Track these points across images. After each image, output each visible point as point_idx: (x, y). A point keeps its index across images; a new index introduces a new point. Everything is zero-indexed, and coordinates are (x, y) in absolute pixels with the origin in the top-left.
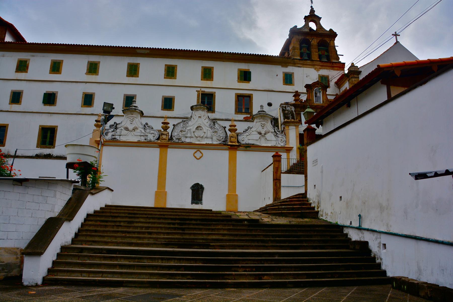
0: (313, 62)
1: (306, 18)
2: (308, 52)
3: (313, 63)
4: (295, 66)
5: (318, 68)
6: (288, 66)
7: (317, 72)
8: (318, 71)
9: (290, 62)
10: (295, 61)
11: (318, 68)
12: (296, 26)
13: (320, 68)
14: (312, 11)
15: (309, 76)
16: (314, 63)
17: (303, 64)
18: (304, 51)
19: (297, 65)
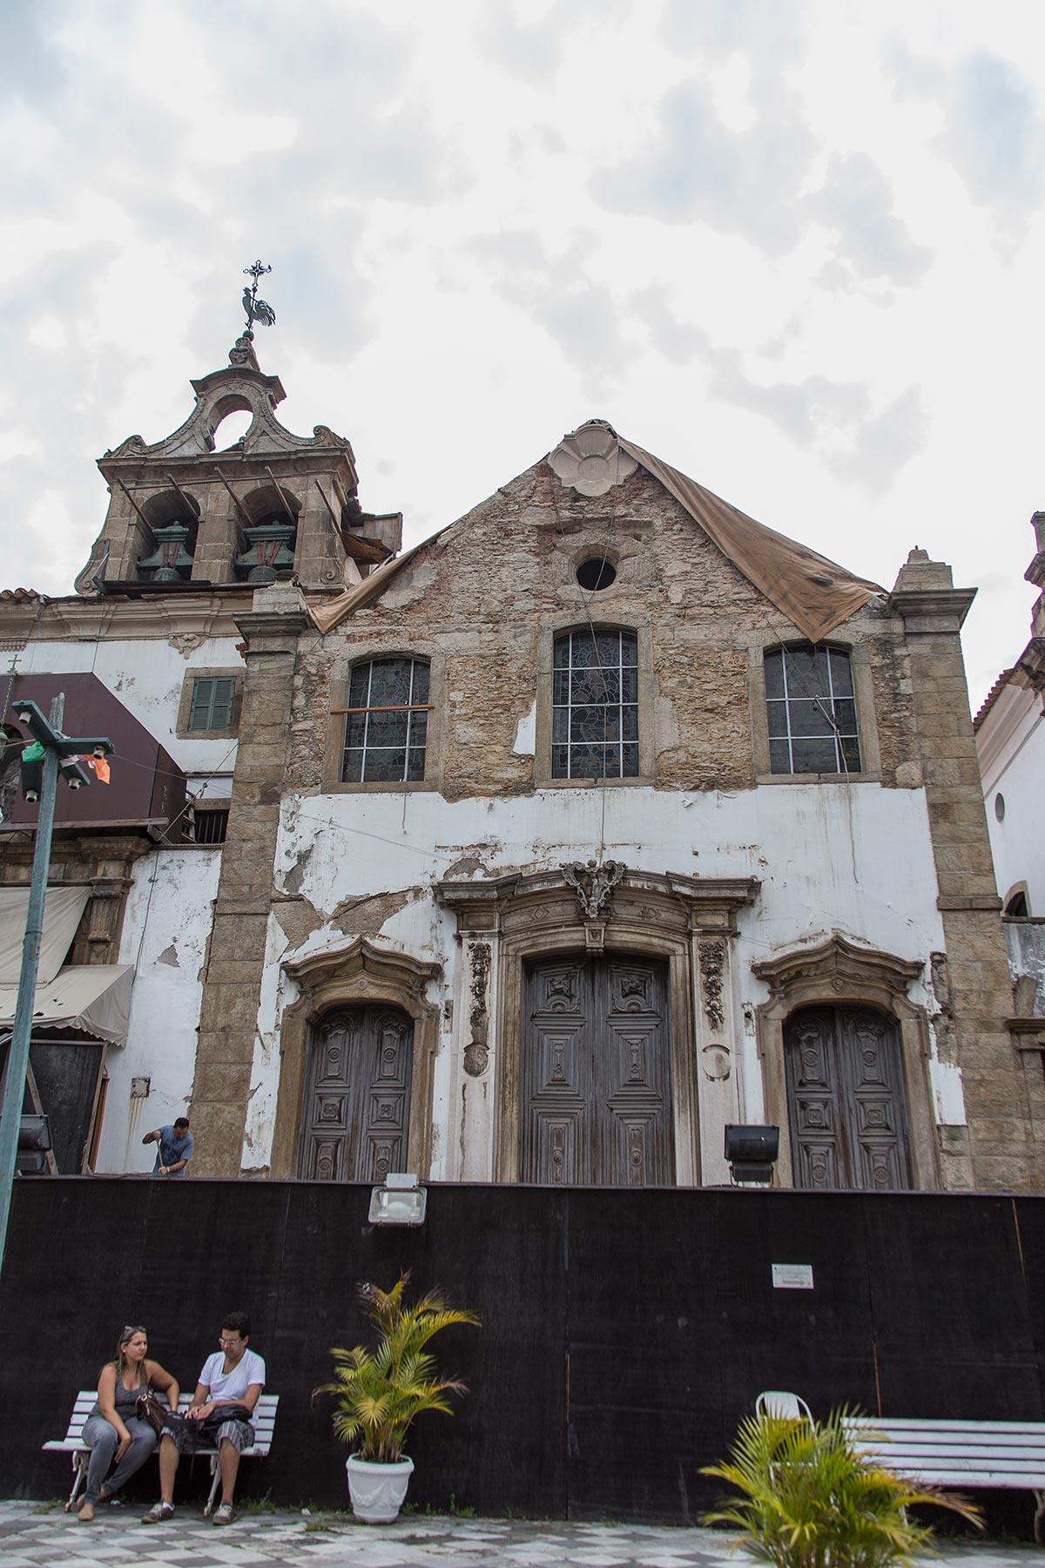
0: (159, 606)
1: (202, 386)
2: (184, 561)
3: (160, 611)
4: (62, 639)
5: (191, 636)
6: (26, 640)
7: (182, 656)
8: (187, 646)
9: (32, 619)
10: (60, 613)
11: (186, 636)
12: (136, 441)
13: (203, 635)
14: (243, 351)
15: (131, 682)
16: (165, 610)
17: (111, 625)
18: (166, 555)
19: (75, 632)
